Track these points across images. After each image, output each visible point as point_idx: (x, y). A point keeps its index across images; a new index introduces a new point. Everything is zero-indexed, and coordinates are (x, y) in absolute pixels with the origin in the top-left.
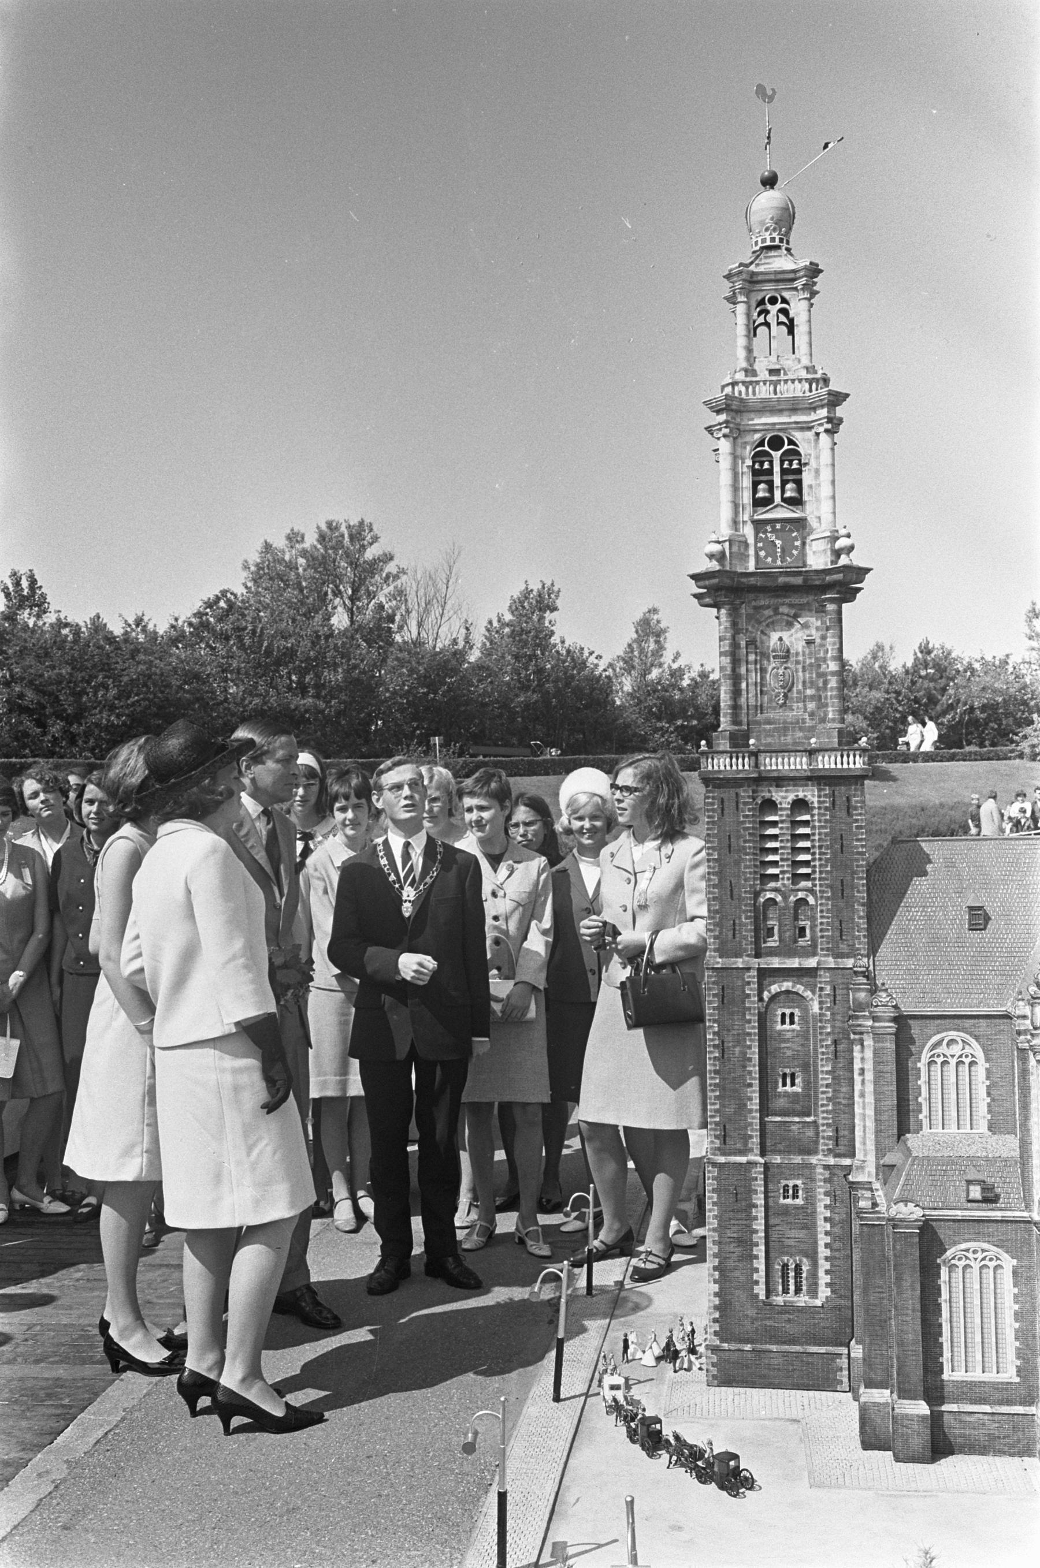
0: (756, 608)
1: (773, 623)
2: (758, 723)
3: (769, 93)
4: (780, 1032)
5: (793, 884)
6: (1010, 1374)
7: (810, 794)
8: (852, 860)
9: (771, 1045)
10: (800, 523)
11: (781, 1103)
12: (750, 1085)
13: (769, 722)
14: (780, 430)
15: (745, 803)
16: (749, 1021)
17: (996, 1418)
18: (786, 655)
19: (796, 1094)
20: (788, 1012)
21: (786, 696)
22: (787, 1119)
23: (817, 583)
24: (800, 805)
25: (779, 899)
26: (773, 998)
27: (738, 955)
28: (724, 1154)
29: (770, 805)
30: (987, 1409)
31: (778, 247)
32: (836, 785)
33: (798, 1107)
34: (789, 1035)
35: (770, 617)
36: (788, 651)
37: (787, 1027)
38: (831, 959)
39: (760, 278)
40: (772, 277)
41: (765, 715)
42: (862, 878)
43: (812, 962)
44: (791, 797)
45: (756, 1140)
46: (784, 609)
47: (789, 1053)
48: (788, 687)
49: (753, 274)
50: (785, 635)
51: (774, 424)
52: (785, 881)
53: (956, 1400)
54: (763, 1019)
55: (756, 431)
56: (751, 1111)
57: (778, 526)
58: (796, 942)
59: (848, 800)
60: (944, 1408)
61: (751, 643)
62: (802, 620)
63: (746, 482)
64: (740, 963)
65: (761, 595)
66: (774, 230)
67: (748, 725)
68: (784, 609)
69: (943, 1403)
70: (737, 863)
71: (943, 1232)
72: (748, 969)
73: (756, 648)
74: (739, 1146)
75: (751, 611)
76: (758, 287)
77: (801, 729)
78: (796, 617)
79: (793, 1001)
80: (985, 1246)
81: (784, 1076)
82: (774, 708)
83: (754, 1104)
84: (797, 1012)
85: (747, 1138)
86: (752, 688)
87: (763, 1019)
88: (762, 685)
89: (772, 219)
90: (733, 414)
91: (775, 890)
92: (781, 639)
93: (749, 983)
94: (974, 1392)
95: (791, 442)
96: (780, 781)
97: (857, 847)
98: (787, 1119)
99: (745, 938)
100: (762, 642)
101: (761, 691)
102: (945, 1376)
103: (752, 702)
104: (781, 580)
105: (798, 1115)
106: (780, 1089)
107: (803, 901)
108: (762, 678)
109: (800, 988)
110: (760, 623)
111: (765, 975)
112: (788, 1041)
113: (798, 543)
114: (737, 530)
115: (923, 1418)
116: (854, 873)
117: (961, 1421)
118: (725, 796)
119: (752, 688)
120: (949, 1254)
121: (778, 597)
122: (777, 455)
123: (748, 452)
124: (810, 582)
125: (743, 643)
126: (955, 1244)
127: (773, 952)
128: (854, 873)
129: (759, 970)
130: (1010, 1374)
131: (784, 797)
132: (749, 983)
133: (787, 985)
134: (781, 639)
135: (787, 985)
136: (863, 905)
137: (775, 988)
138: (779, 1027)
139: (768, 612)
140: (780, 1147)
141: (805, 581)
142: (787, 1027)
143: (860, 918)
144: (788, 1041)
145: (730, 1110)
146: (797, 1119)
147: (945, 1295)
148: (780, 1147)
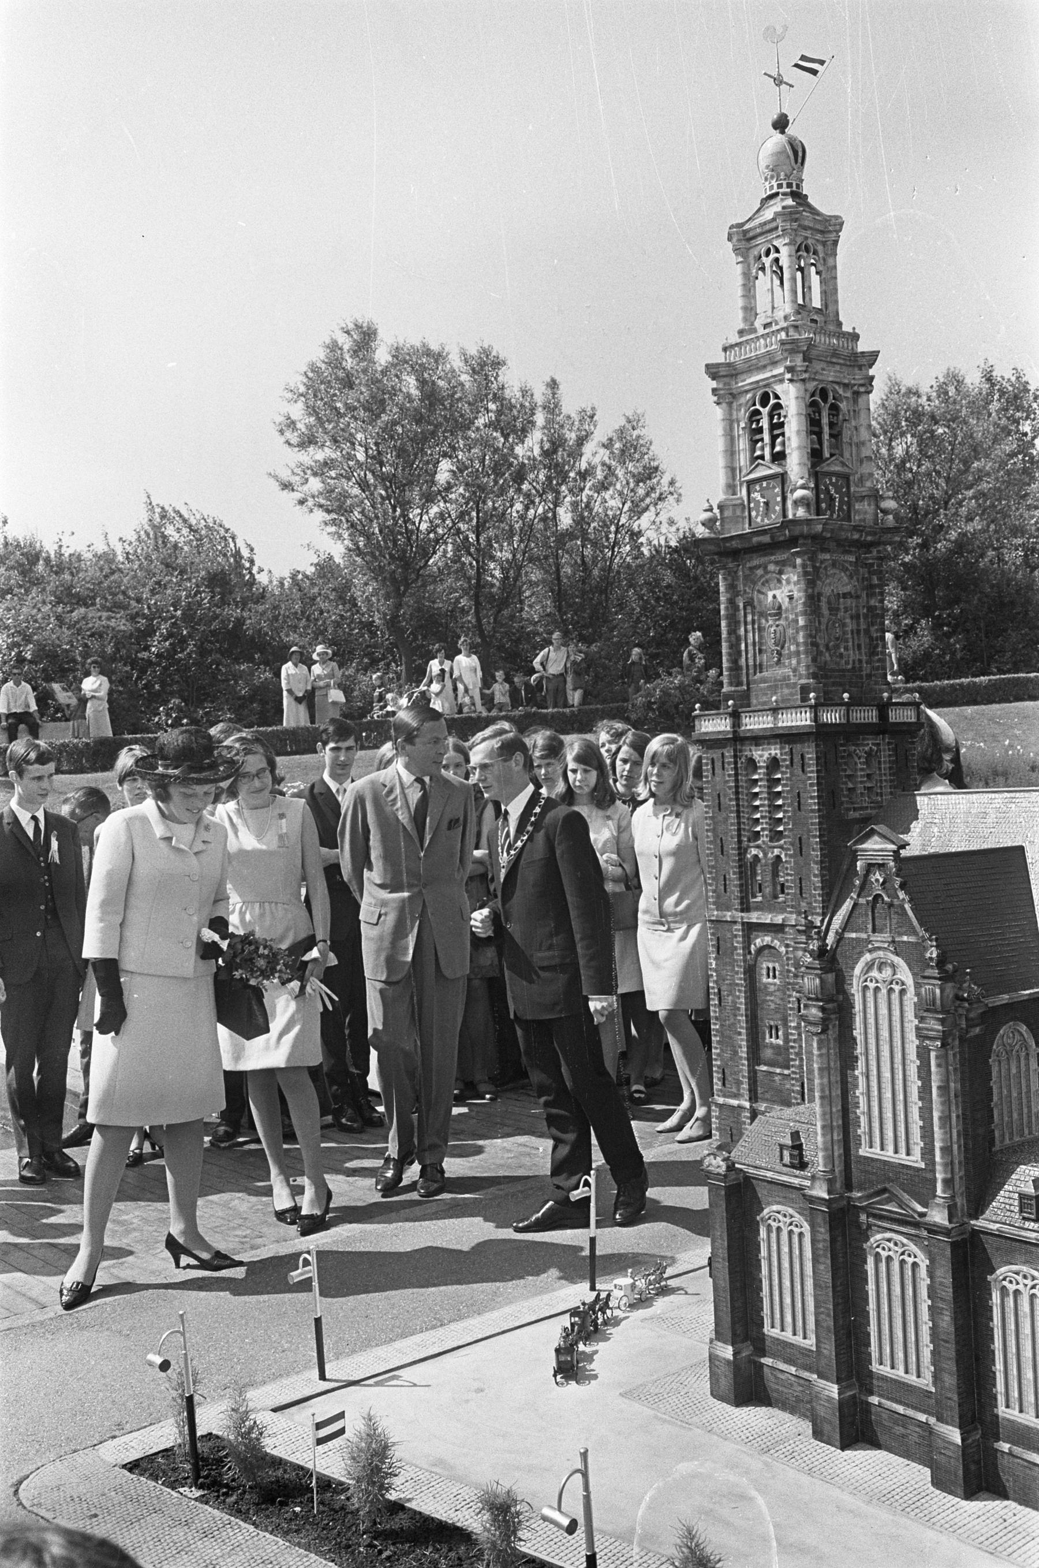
0: (751, 569)
1: (767, 581)
2: (755, 682)
3: (779, 30)
4: (766, 985)
5: (771, 841)
6: (107, 1242)
7: (775, 751)
8: (806, 818)
9: (761, 996)
10: (783, 477)
11: (768, 1054)
12: (740, 1034)
13: (764, 680)
14: (765, 386)
15: (729, 763)
16: (737, 973)
17: (802, 1382)
18: (779, 611)
19: (778, 1046)
20: (771, 966)
21: (779, 654)
22: (771, 1069)
23: (782, 538)
24: (774, 764)
25: (761, 855)
26: (760, 950)
27: (728, 909)
28: (724, 1096)
29: (752, 764)
30: (793, 1370)
31: (777, 194)
32: (795, 742)
33: (780, 1059)
34: (772, 988)
35: (762, 576)
36: (780, 608)
37: (770, 980)
38: (794, 916)
39: (751, 234)
40: (758, 230)
41: (765, 674)
42: (815, 836)
43: (779, 919)
44: (766, 755)
45: (746, 1086)
46: (771, 567)
47: (773, 1006)
48: (781, 643)
49: (745, 232)
50: (777, 593)
51: (757, 382)
52: (764, 839)
53: (774, 1356)
54: (751, 972)
55: (747, 392)
56: (741, 1058)
57: (765, 484)
58: (776, 897)
59: (802, 757)
60: (763, 1360)
61: (749, 603)
62: (784, 577)
63: (743, 444)
64: (728, 916)
65: (754, 555)
66: (772, 177)
67: (748, 684)
68: (771, 567)
69: (764, 1356)
70: (726, 819)
71: (762, 1192)
72: (735, 922)
73: (753, 607)
74: (734, 1090)
75: (747, 572)
76: (754, 242)
77: (788, 686)
78: (781, 572)
79: (772, 955)
80: (791, 1211)
81: (771, 1027)
82: (771, 666)
83: (743, 1052)
84: (777, 965)
85: (739, 1083)
86: (750, 648)
87: (751, 972)
88: (761, 644)
89: (767, 167)
90: (726, 380)
91: (758, 847)
92: (774, 597)
93: (736, 936)
94: (788, 1352)
95: (777, 397)
96: (758, 739)
97: (810, 805)
98: (771, 1069)
99: (733, 892)
100: (760, 602)
101: (760, 651)
102: (765, 1330)
103: (751, 662)
104: (755, 540)
105: (781, 1067)
106: (767, 1040)
107: (778, 857)
108: (760, 637)
109: (776, 943)
110: (755, 583)
111: (751, 929)
112: (771, 994)
113: (779, 499)
114: (734, 494)
115: (728, 1361)
116: (809, 831)
117: (776, 1378)
118: (715, 756)
119: (750, 648)
120: (766, 1211)
121: (765, 555)
122: (765, 411)
123: (743, 415)
124: (777, 539)
125: (741, 605)
126: (769, 1204)
127: (759, 907)
128: (809, 831)
129: (743, 924)
130: (107, 1242)
131: (762, 755)
132: (736, 936)
133: (768, 939)
134: (774, 597)
135: (768, 939)
136: (816, 863)
137: (758, 942)
138: (765, 980)
139: (760, 572)
140: (768, 1096)
141: (772, 538)
142: (770, 980)
143: (815, 876)
144: (771, 994)
145: (727, 1055)
146: (778, 1071)
147: (764, 1253)
148: (768, 1096)
